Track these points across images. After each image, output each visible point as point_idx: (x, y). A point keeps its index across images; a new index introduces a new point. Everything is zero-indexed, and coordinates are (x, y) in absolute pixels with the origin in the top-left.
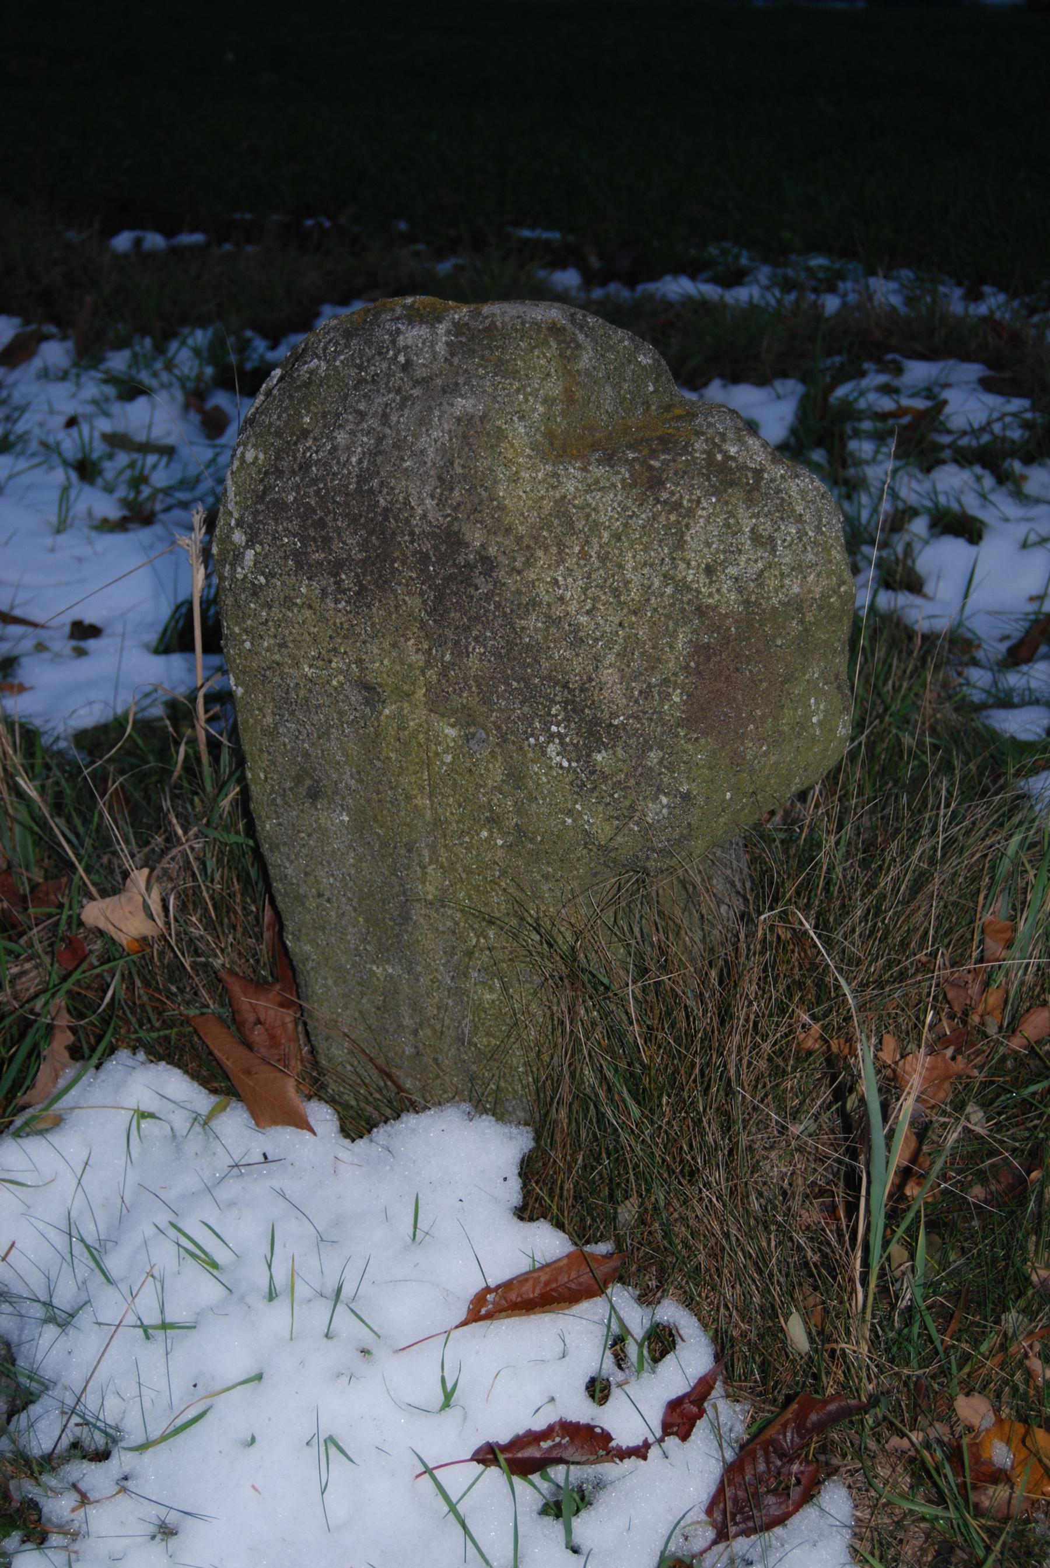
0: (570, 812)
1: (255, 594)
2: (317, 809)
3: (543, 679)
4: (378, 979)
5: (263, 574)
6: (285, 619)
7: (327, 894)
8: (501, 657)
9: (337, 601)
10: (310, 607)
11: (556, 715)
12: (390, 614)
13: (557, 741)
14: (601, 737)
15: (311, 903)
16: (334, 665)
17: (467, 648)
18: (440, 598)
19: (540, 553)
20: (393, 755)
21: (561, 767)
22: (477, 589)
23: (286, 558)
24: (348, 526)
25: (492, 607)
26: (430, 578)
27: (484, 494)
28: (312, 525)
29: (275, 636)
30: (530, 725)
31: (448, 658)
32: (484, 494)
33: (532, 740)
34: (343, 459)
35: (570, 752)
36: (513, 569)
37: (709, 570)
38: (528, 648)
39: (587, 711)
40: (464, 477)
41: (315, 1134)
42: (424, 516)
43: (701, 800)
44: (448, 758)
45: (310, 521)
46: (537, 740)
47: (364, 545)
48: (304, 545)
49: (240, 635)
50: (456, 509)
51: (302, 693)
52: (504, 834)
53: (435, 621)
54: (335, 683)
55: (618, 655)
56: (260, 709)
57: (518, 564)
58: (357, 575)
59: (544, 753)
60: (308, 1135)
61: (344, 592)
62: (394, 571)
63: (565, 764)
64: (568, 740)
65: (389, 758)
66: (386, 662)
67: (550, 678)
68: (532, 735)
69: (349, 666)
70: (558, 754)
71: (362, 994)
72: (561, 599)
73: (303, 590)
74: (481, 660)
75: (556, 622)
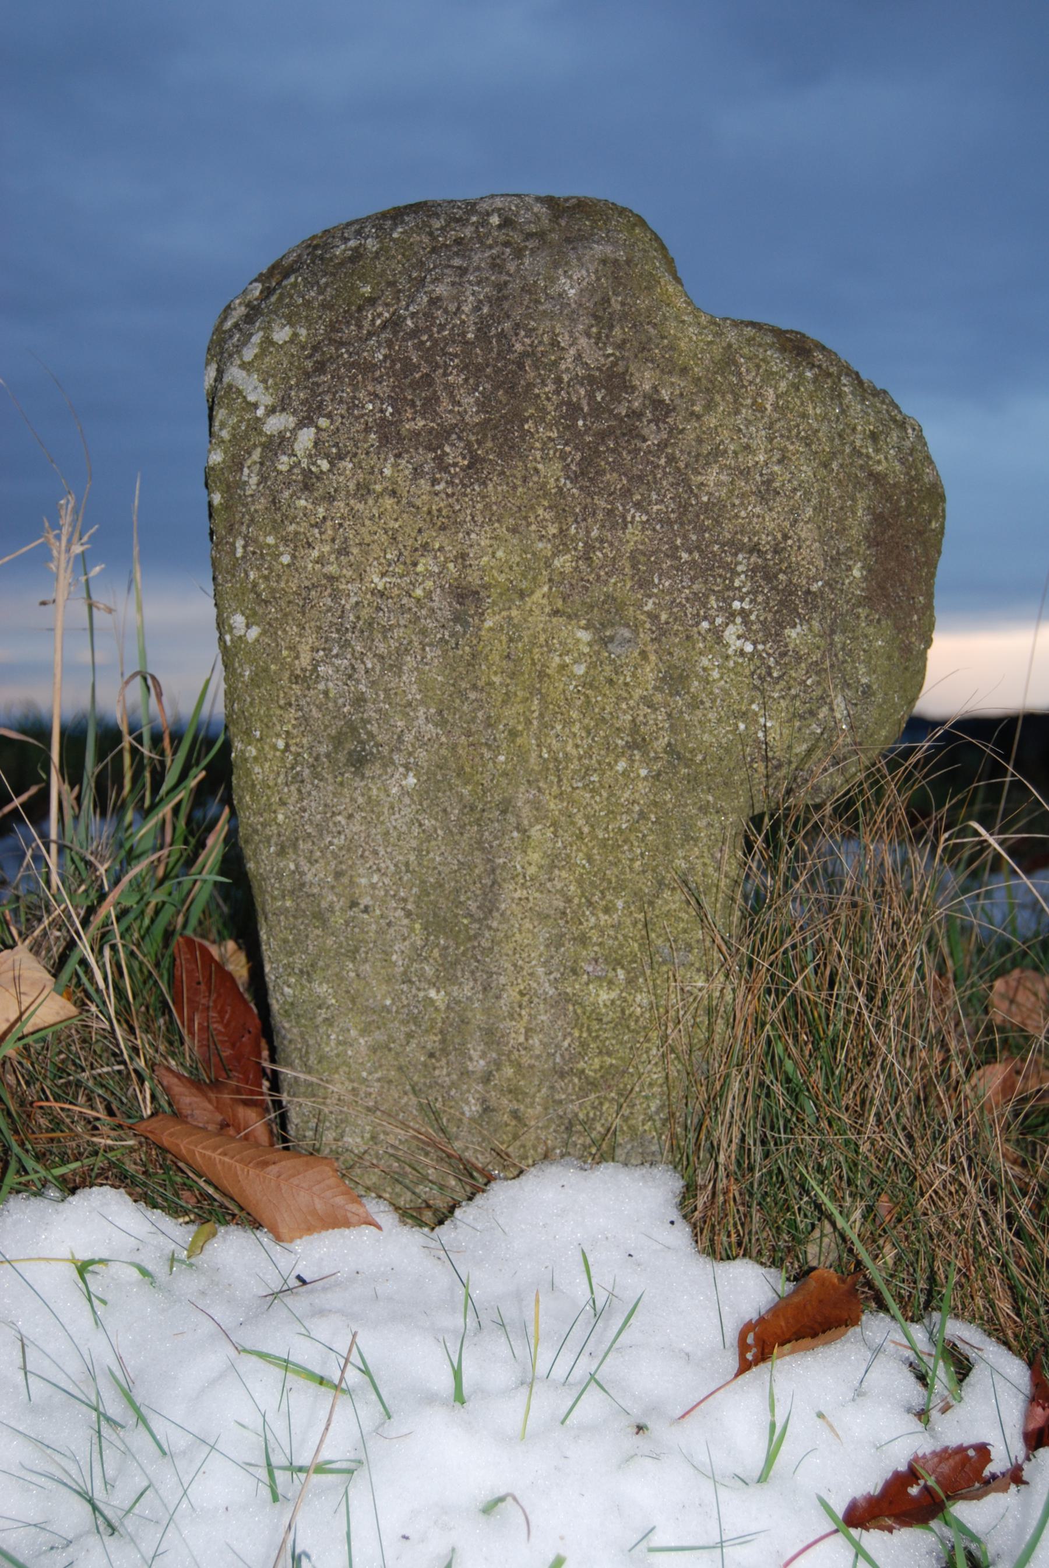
0: (744, 715)
1: (307, 487)
2: (363, 777)
3: (723, 545)
4: (437, 1009)
5: (327, 456)
6: (353, 514)
7: (366, 901)
8: (670, 523)
9: (434, 482)
10: (394, 493)
11: (739, 589)
12: (515, 488)
13: (738, 620)
14: (796, 609)
15: (337, 920)
16: (420, 568)
17: (624, 517)
18: (586, 463)
19: (718, 398)
20: (497, 679)
21: (742, 653)
22: (645, 440)
23: (367, 430)
24: (466, 380)
25: (663, 461)
26: (579, 434)
27: (653, 332)
28: (410, 385)
29: (333, 540)
30: (704, 605)
31: (595, 533)
32: (653, 332)
33: (705, 625)
34: (452, 307)
35: (756, 632)
36: (692, 413)
37: (874, 436)
38: (707, 508)
39: (781, 576)
40: (624, 317)
41: (380, 1228)
42: (578, 357)
43: (879, 698)
44: (580, 670)
45: (408, 381)
46: (712, 623)
47: (482, 406)
48: (397, 411)
49: (277, 546)
50: (620, 346)
51: (365, 613)
52: (648, 762)
53: (581, 489)
54: (419, 592)
55: (815, 509)
56: (292, 648)
57: (697, 408)
58: (469, 445)
59: (719, 639)
60: (368, 1231)
61: (445, 469)
62: (524, 434)
63: (749, 648)
64: (753, 617)
65: (490, 684)
66: (500, 554)
67: (731, 543)
68: (705, 618)
69: (444, 566)
70: (739, 637)
71: (410, 1036)
72: (747, 447)
73: (387, 472)
74: (643, 530)
75: (745, 473)
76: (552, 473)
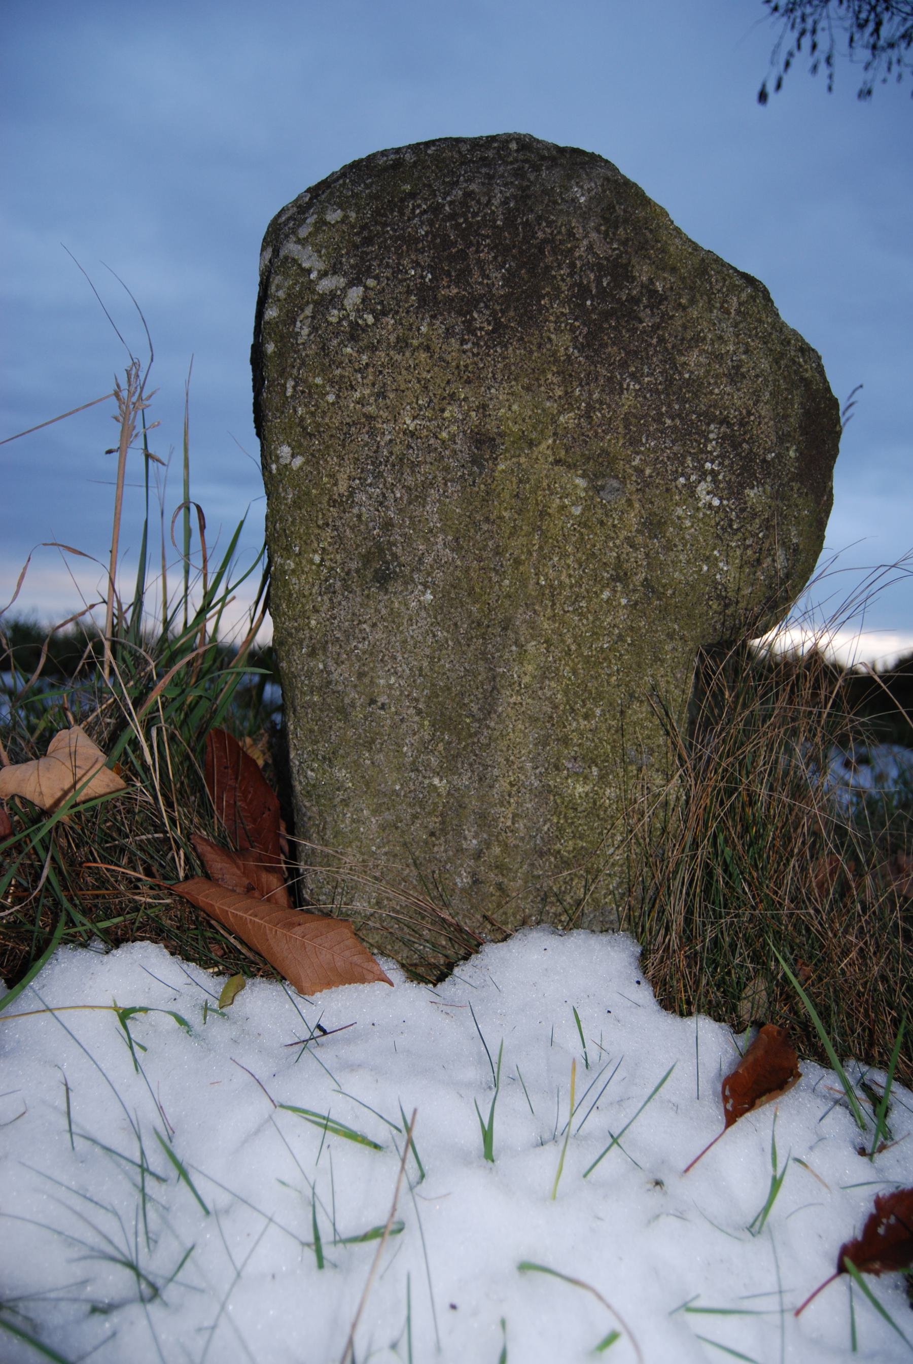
0: (707, 559)
1: (353, 338)
3: (699, 415)
4: (439, 795)
5: (373, 311)
6: (393, 364)
9: (463, 342)
10: (428, 348)
11: (711, 453)
12: (531, 352)
13: (709, 478)
15: (358, 715)
16: (447, 414)
20: (506, 514)
21: (710, 506)
22: (641, 322)
23: (409, 292)
24: (495, 258)
25: (655, 341)
27: (649, 236)
29: (373, 385)
30: (682, 463)
31: (596, 396)
32: (649, 236)
33: (682, 480)
34: (484, 200)
35: (723, 489)
36: (680, 304)
39: (745, 446)
41: (392, 984)
42: (590, 248)
44: (577, 511)
45: (446, 253)
46: (688, 479)
47: (507, 281)
49: (324, 386)
50: (625, 243)
51: (397, 449)
53: (587, 357)
54: (444, 435)
56: (332, 476)
57: (683, 301)
58: (494, 313)
61: (473, 332)
63: (716, 502)
64: (720, 477)
65: (501, 518)
66: (515, 407)
67: (705, 414)
68: (682, 475)
69: (467, 415)
70: (708, 493)
71: (415, 817)
72: (720, 338)
73: (424, 329)
74: (636, 397)
75: (719, 358)
76: (562, 343)
